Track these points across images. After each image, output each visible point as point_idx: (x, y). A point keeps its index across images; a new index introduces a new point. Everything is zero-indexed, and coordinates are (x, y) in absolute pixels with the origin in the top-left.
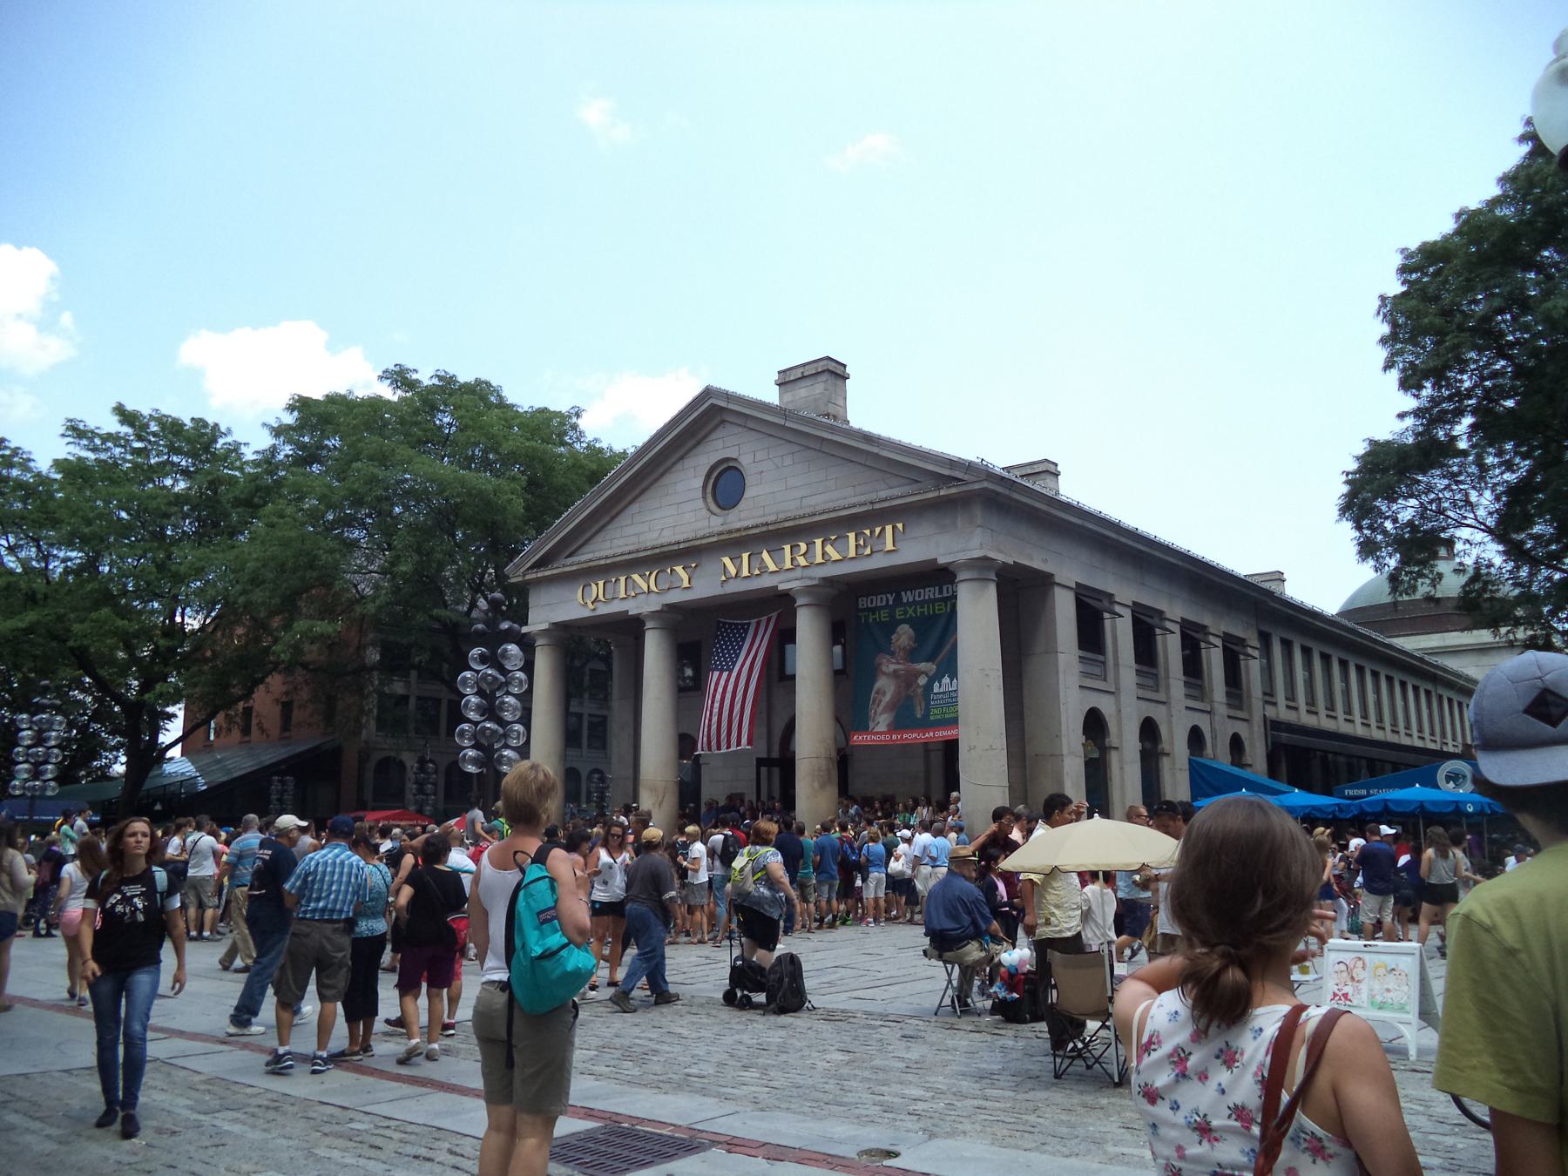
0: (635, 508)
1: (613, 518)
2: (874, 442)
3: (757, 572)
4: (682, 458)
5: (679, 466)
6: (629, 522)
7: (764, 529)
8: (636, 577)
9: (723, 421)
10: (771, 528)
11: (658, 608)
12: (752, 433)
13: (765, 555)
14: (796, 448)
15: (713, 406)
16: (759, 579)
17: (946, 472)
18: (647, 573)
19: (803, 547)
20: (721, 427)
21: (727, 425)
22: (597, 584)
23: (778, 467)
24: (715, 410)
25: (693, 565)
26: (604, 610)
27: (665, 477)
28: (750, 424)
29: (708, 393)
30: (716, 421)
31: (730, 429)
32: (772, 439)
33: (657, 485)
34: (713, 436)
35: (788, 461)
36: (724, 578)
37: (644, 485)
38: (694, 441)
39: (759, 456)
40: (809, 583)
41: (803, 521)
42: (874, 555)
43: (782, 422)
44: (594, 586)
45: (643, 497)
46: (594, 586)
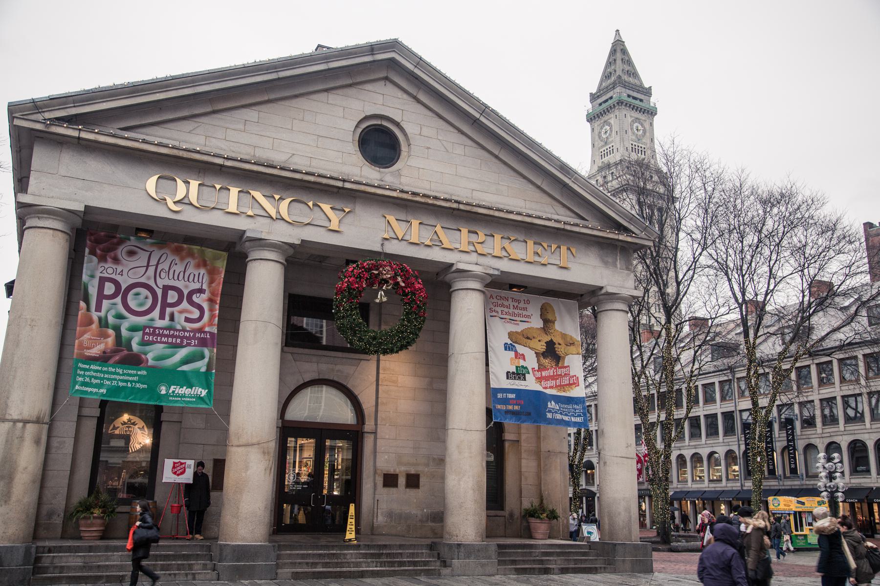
0: (251, 114)
1: (214, 112)
2: (569, 174)
3: (428, 242)
4: (326, 90)
5: (323, 96)
6: (241, 127)
7: (455, 206)
8: (257, 195)
9: (386, 79)
10: (462, 207)
11: (298, 242)
12: (419, 106)
13: (438, 229)
14: (469, 142)
15: (392, 60)
16: (428, 250)
17: (625, 224)
18: (277, 197)
19: (482, 237)
20: (382, 83)
21: (388, 83)
22: (187, 183)
23: (447, 151)
24: (392, 63)
25: (347, 210)
26: (190, 216)
27: (298, 100)
28: (422, 97)
29: (394, 45)
30: (382, 74)
31: (390, 89)
32: (441, 122)
33: (287, 103)
34: (368, 87)
35: (459, 150)
36: (386, 236)
37: (273, 96)
38: (349, 82)
39: (425, 131)
40: (491, 272)
41: (497, 214)
42: (549, 266)
43: (477, 115)
44: (180, 183)
45: (263, 108)
46: (180, 183)
